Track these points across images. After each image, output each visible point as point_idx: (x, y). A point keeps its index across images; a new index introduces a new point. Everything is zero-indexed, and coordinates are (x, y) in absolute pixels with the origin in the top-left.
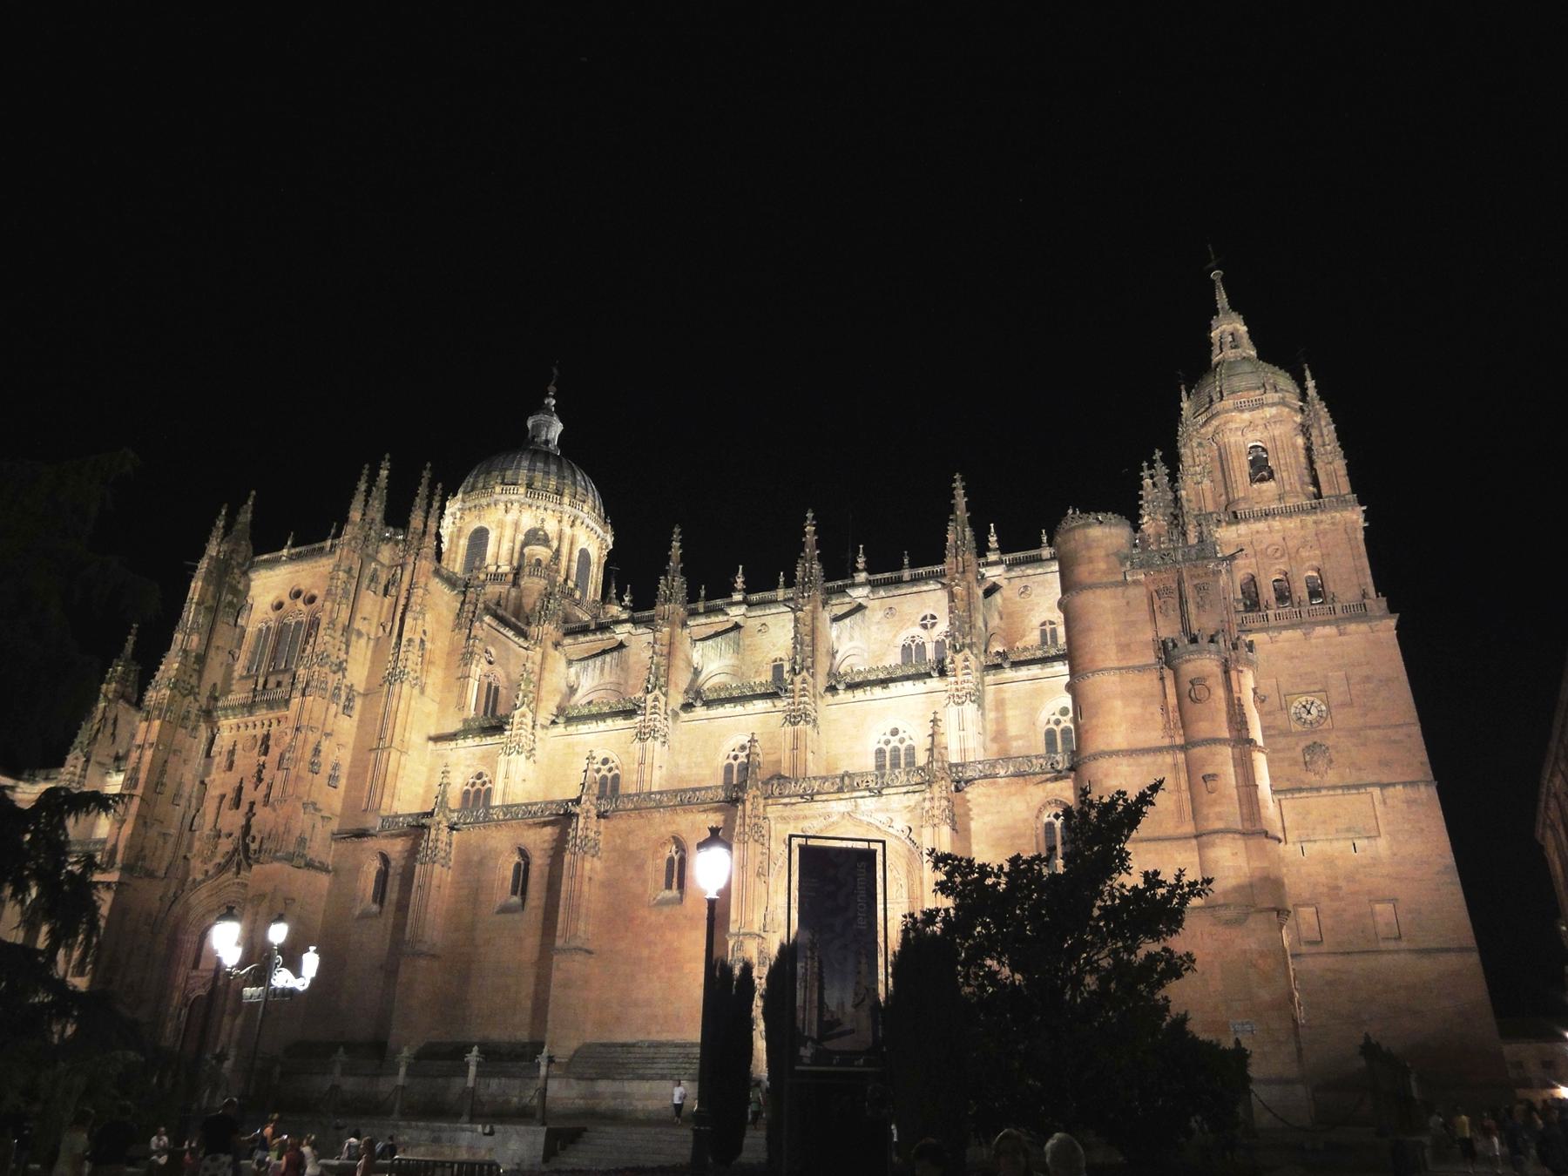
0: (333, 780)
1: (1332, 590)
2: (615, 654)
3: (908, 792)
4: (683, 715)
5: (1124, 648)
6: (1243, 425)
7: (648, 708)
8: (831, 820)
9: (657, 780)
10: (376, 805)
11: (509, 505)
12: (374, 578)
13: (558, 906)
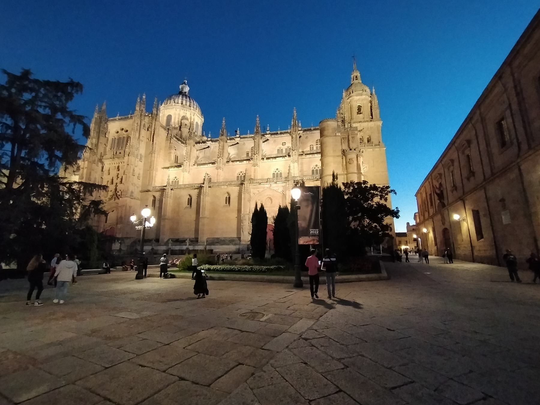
0: (138, 178)
2: (207, 149)
4: (227, 164)
8: (265, 189)
9: (221, 179)
12: (144, 125)
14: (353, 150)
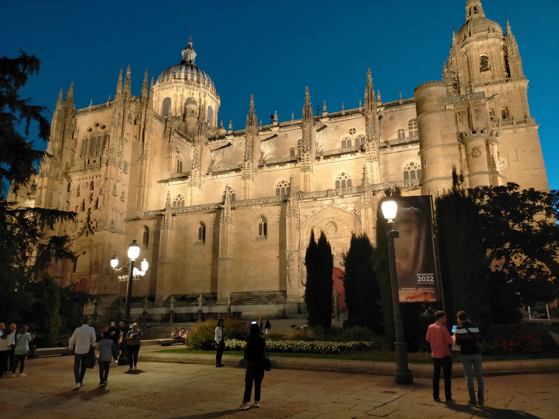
1: (512, 115)
3: (354, 196)
5: (444, 136)
6: (479, 47)
7: (246, 167)
9: (251, 195)
10: (141, 207)
11: (178, 88)
13: (218, 243)
14: (479, 133)
